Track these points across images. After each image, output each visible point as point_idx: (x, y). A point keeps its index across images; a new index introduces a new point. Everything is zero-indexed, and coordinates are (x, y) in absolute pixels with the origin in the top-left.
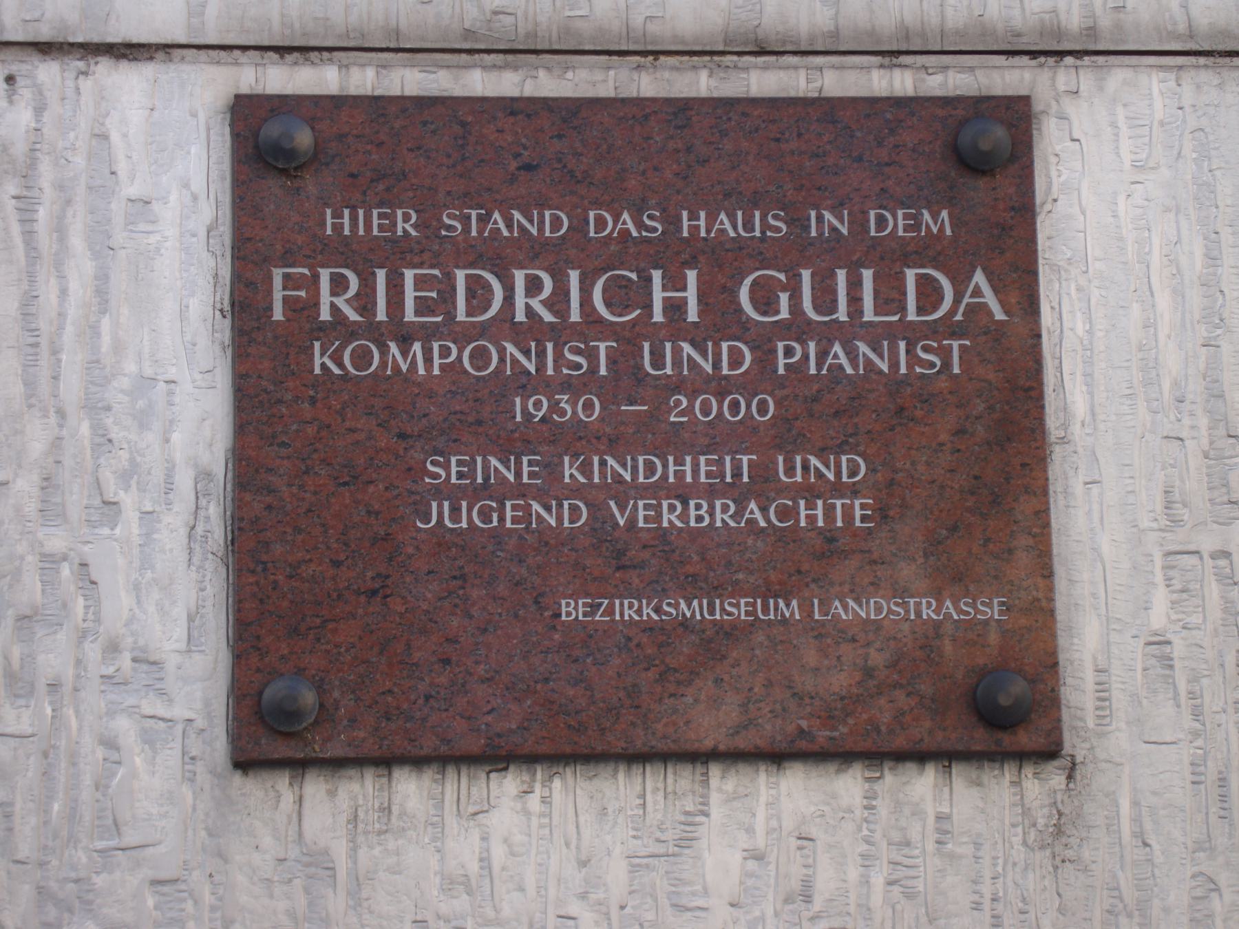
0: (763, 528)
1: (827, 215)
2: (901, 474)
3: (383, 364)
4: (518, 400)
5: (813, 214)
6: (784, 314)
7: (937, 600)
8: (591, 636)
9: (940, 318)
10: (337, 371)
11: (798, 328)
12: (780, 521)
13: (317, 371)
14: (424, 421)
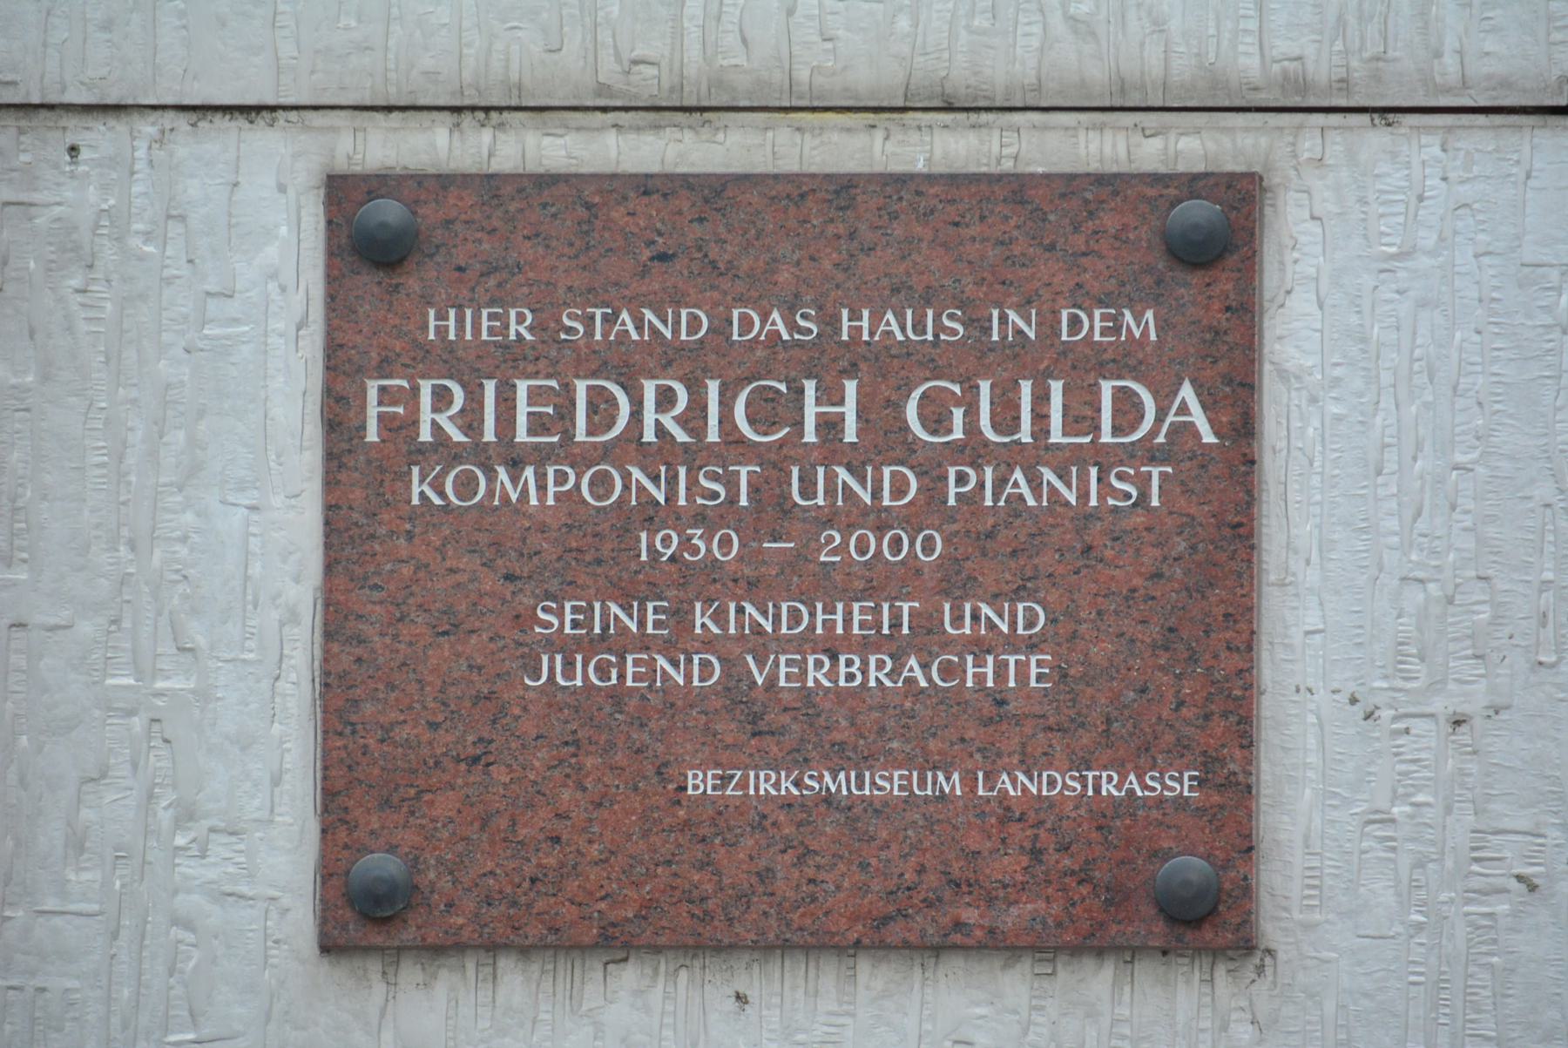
0: (923, 691)
1: (1012, 316)
2: (1084, 626)
3: (490, 493)
4: (644, 536)
5: (995, 313)
6: (958, 434)
8: (720, 813)
10: (437, 501)
11: (973, 451)
12: (943, 680)
13: (415, 501)
14: (535, 559)
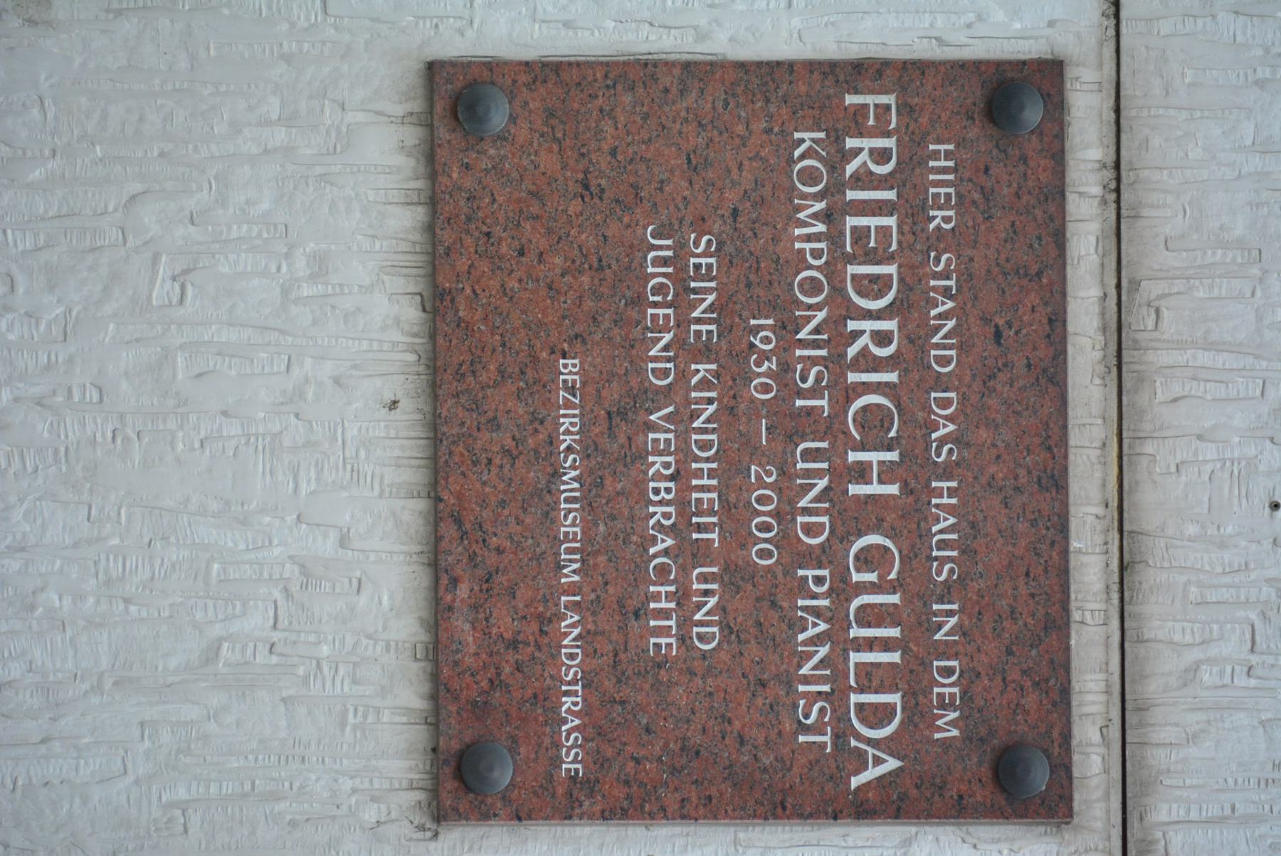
0: (646, 551)
1: (953, 621)
2: (700, 682)
3: (804, 196)
4: (770, 322)
5: (955, 607)
6: (856, 577)
7: (580, 711)
8: (544, 386)
9: (852, 725)
10: (797, 153)
11: (842, 590)
12: (655, 567)
13: (797, 135)
14: (750, 234)
